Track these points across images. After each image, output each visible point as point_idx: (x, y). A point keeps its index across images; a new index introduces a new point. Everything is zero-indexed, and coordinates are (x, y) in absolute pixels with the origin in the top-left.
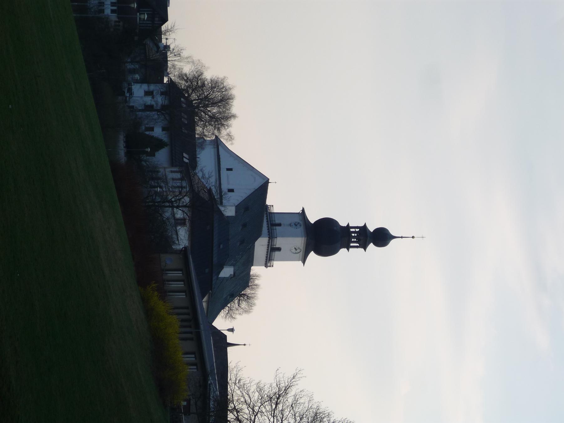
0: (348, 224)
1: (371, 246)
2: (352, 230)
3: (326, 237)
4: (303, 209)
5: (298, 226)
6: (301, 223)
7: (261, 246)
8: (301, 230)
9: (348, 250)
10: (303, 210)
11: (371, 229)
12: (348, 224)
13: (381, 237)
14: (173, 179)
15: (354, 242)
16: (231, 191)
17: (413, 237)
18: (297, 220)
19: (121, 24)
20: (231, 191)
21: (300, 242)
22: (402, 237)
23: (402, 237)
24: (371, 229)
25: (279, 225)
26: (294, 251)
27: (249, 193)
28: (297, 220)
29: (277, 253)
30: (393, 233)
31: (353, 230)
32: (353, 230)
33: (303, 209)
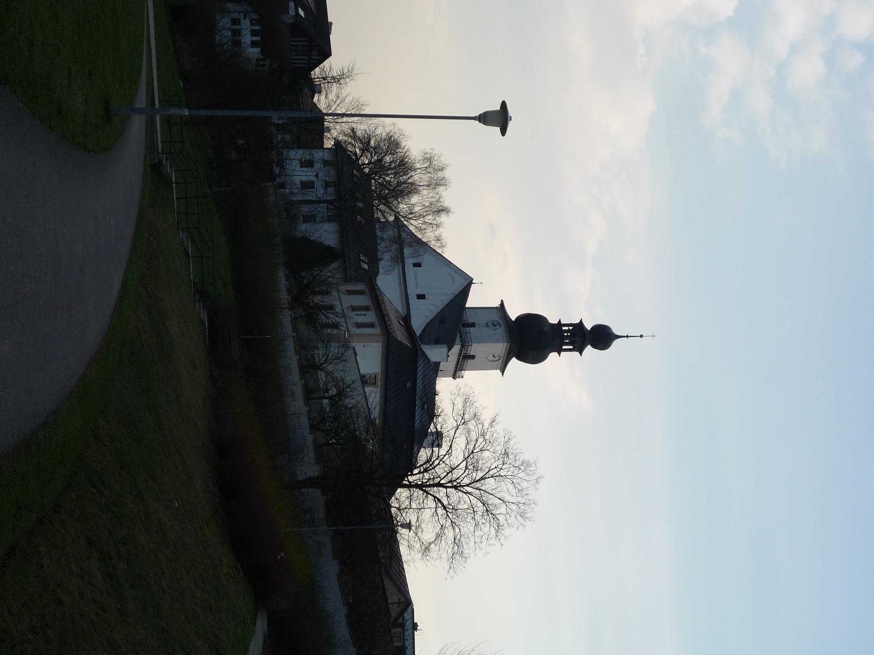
1: (589, 349)
2: (564, 328)
3: (532, 338)
5: (497, 326)
6: (501, 321)
8: (501, 332)
13: (601, 337)
14: (354, 309)
15: (567, 344)
16: (421, 297)
17: (641, 336)
18: (496, 317)
20: (421, 297)
21: (500, 348)
22: (627, 337)
23: (627, 337)
25: (473, 325)
26: (492, 358)
28: (496, 317)
30: (616, 332)
31: (566, 328)
32: (566, 328)
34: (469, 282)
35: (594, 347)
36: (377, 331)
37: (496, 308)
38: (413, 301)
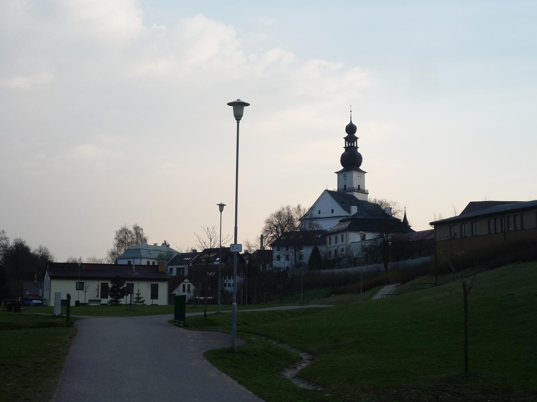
3: (351, 160)
7: (359, 196)
8: (348, 174)
11: (346, 135)
13: (351, 129)
14: (336, 242)
16: (332, 211)
18: (342, 176)
19: (241, 273)
20: (332, 211)
21: (355, 174)
24: (346, 135)
25: (345, 186)
27: (334, 201)
28: (342, 176)
29: (361, 187)
34: (327, 191)
35: (355, 132)
36: (344, 234)
38: (334, 214)
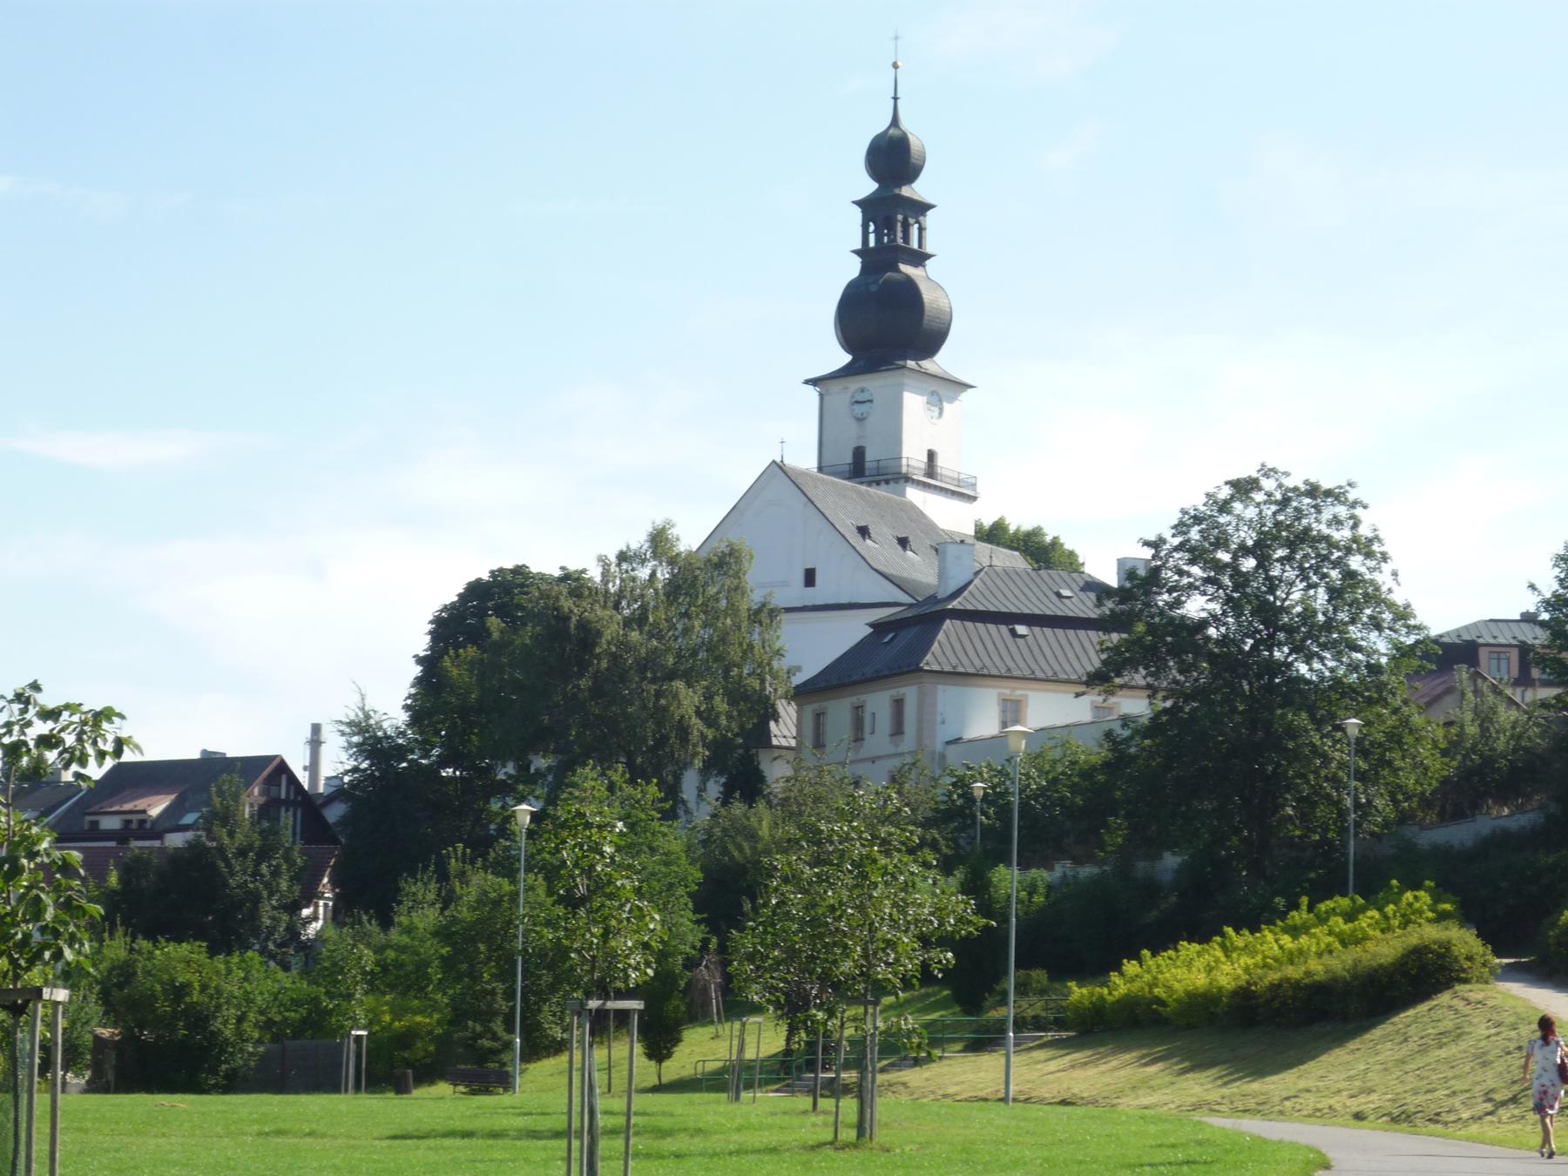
0: (856, 252)
2: (872, 243)
4: (807, 382)
8: (874, 384)
9: (929, 256)
10: (814, 382)
11: (869, 187)
12: (856, 252)
13: (892, 159)
15: (906, 238)
16: (810, 578)
20: (810, 578)
22: (895, 99)
23: (895, 99)
24: (869, 187)
29: (940, 462)
30: (881, 124)
31: (872, 238)
32: (872, 238)
33: (807, 382)
34: (774, 462)
37: (821, 396)
38: (822, 592)
